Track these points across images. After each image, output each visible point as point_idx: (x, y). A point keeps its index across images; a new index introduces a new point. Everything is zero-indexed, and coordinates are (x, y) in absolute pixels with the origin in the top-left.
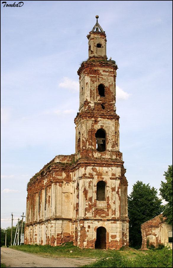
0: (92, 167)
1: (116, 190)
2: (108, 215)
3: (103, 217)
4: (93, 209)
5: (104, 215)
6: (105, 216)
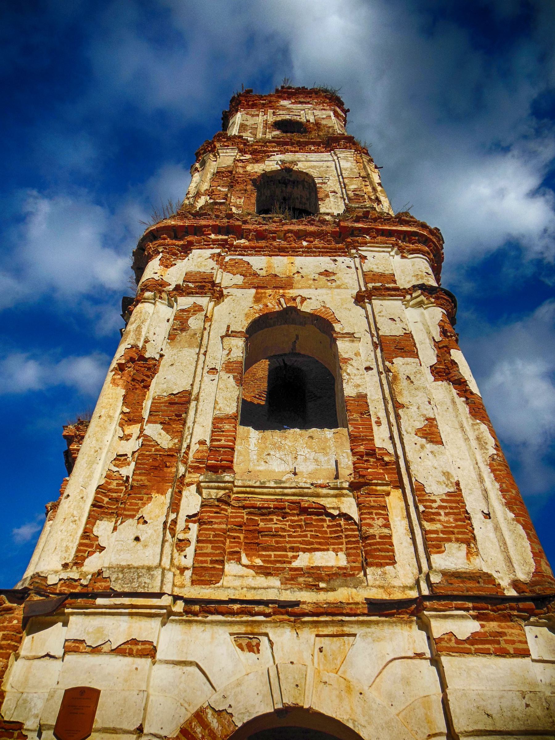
0: (218, 251)
2: (374, 552)
3: (316, 577)
4: (191, 502)
5: (331, 559)
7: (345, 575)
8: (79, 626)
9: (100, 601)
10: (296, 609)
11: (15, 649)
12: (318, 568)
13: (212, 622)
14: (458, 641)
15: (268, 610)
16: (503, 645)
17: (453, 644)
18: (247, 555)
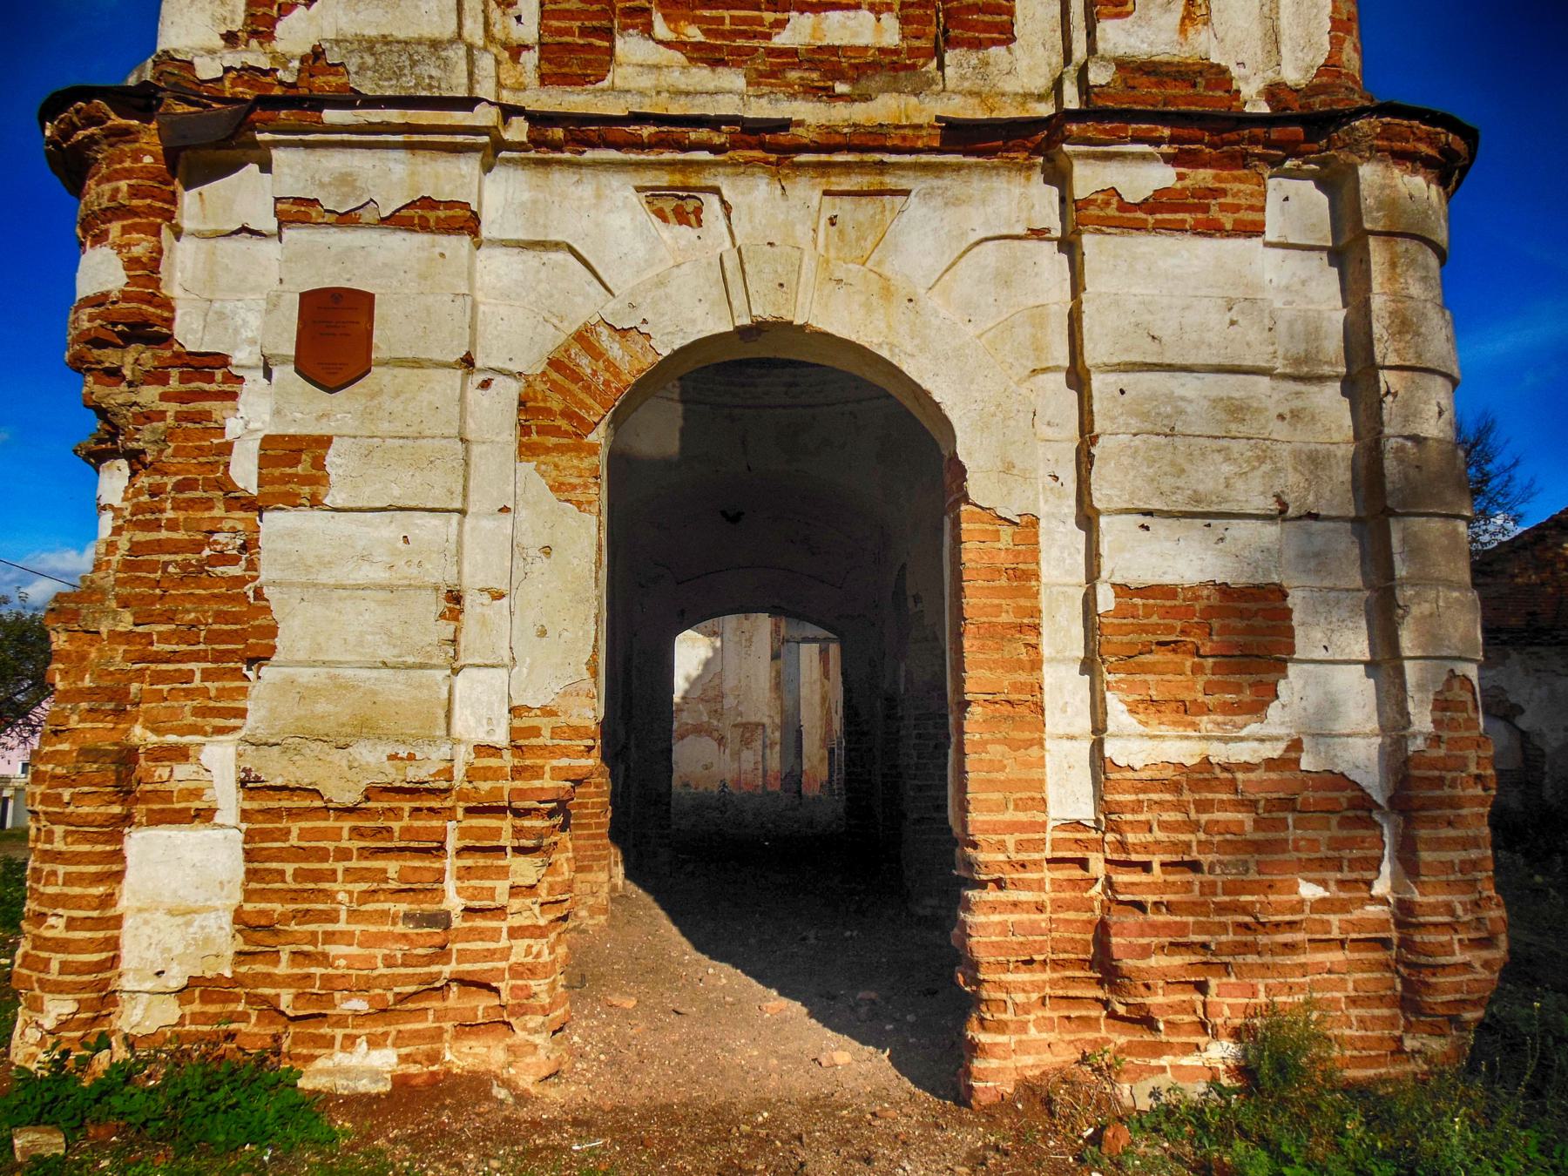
3: (830, 69)
6: (887, 67)
7: (895, 67)
8: (295, 171)
9: (330, 116)
10: (783, 138)
11: (169, 216)
12: (833, 50)
13: (595, 164)
14: (1124, 207)
15: (718, 139)
16: (1215, 213)
17: (1112, 211)
18: (666, 17)
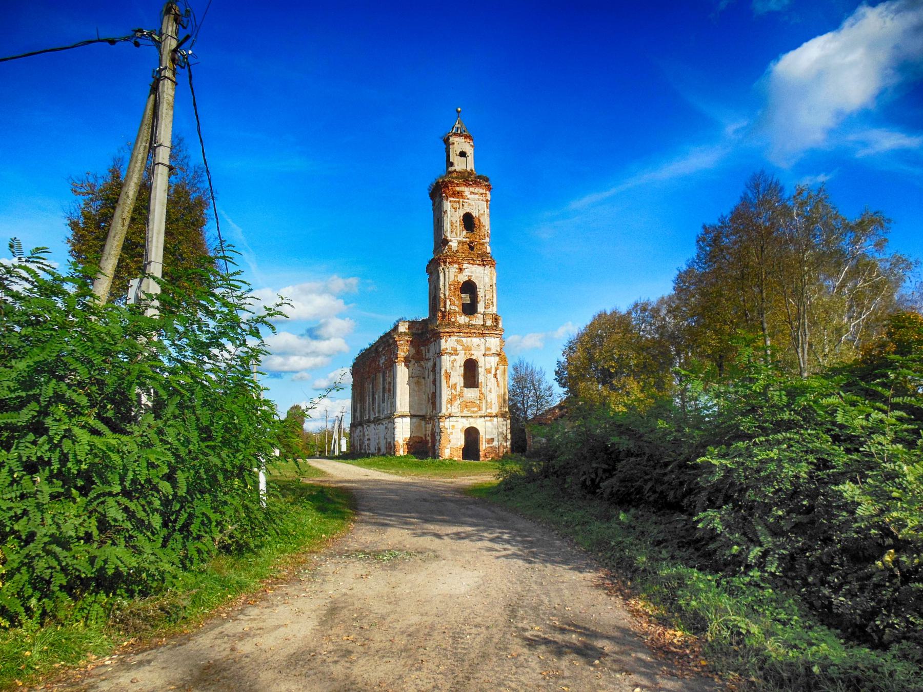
1: (493, 372)
3: (475, 412)
5: (476, 409)
